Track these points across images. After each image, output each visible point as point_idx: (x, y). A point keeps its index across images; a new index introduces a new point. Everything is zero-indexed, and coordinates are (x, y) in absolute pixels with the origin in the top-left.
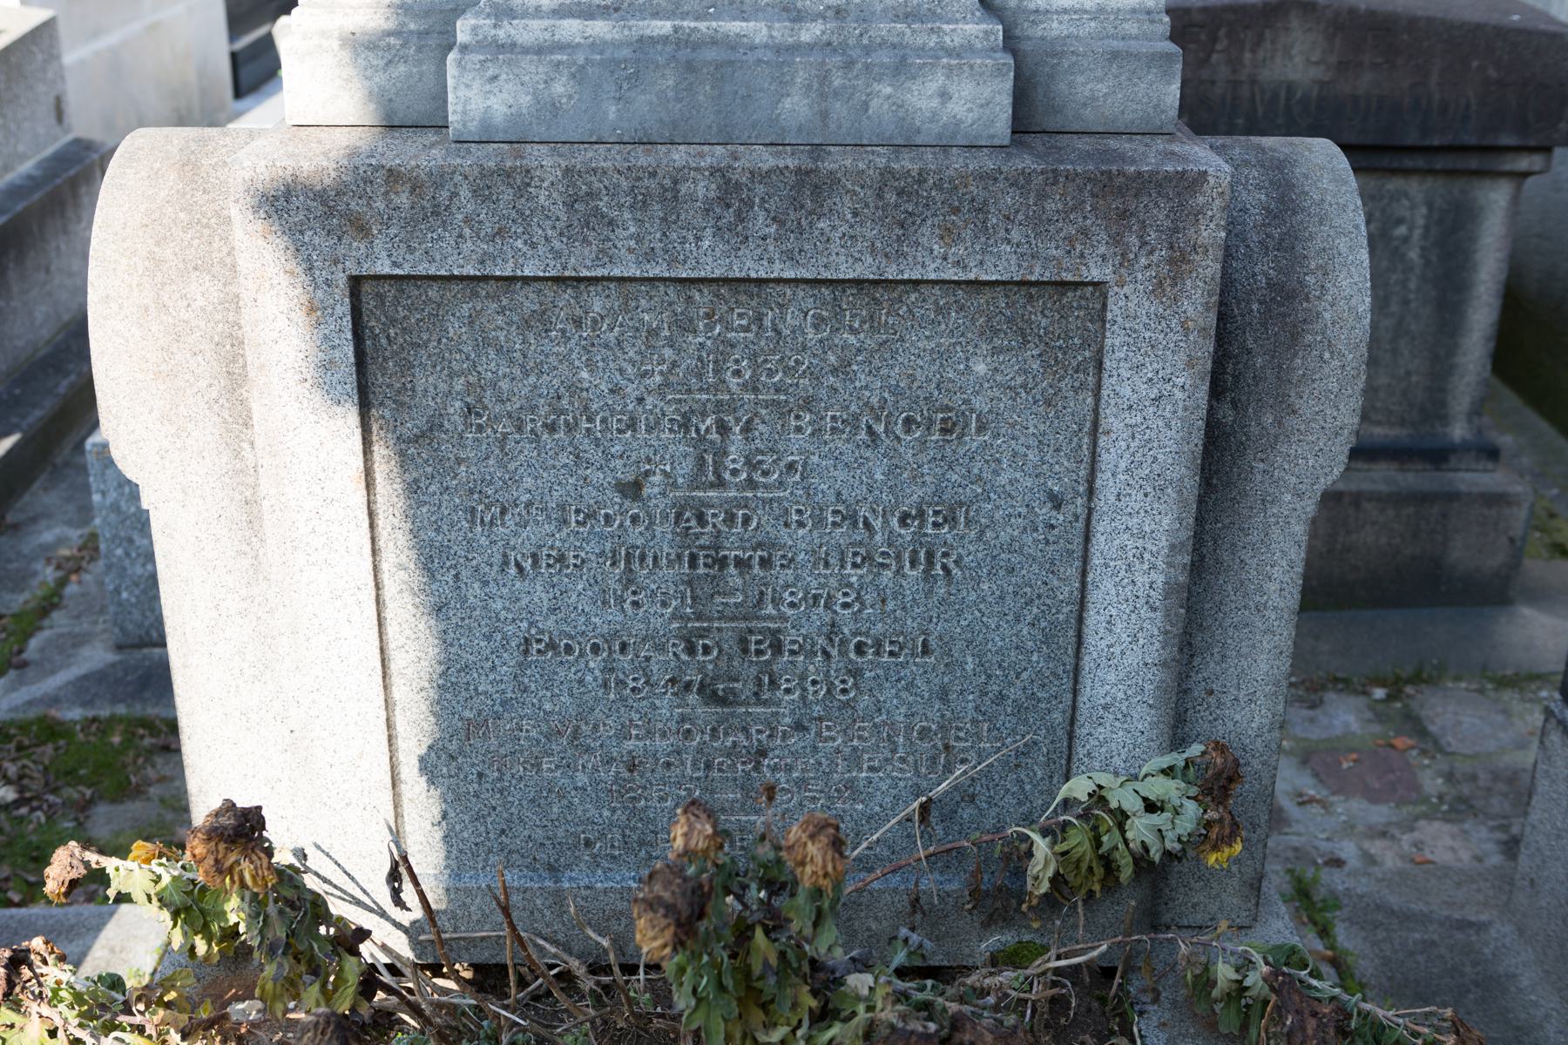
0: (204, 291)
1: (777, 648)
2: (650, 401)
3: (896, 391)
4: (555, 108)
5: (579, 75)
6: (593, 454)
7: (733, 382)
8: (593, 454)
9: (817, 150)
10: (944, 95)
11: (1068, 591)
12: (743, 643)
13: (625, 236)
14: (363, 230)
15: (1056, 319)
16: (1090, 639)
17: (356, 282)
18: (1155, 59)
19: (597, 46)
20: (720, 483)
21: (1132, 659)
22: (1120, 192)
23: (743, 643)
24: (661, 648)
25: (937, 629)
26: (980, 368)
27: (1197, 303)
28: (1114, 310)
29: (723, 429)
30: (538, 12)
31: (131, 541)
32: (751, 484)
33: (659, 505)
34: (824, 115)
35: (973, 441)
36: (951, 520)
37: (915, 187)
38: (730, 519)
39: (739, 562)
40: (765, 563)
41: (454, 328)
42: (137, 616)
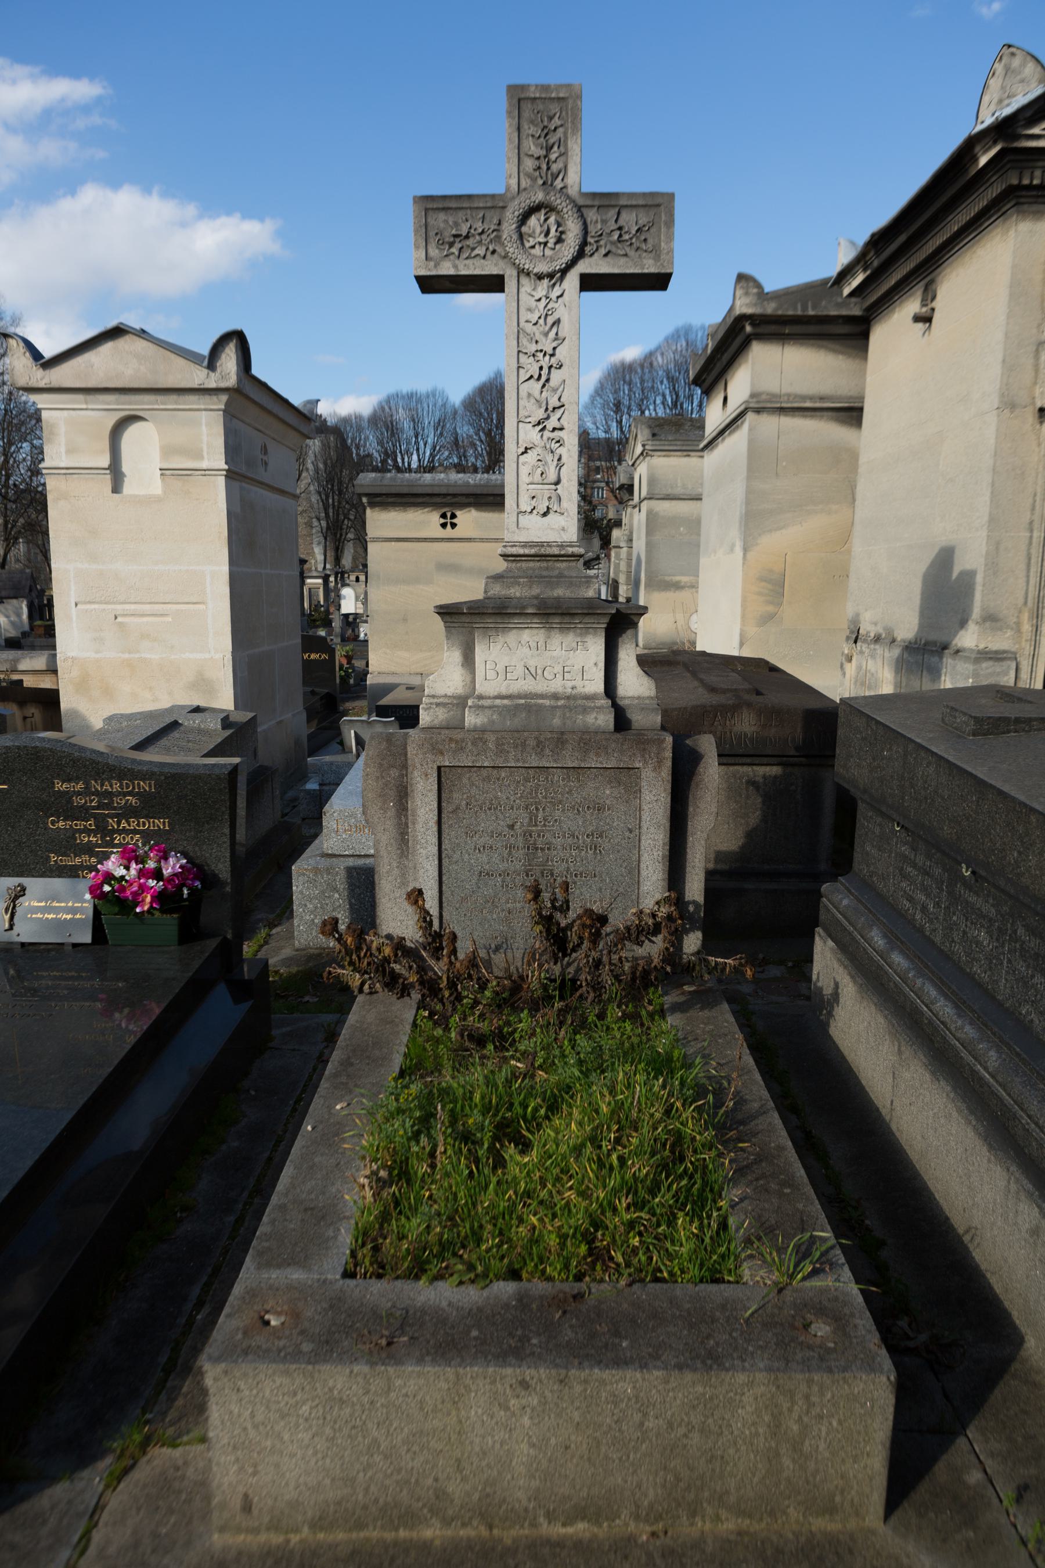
0: (394, 773)
1: (552, 875)
2: (518, 801)
3: (585, 799)
4: (493, 722)
5: (500, 714)
6: (501, 816)
7: (540, 796)
8: (501, 816)
9: (562, 733)
10: (596, 718)
11: (635, 858)
12: (542, 873)
13: (511, 755)
14: (442, 753)
15: (626, 778)
16: (642, 872)
17: (439, 768)
18: (653, 710)
19: (505, 706)
20: (536, 825)
21: (654, 878)
22: (643, 743)
23: (542, 873)
24: (519, 875)
25: (598, 869)
26: (608, 792)
27: (666, 772)
28: (643, 776)
29: (537, 809)
30: (489, 698)
31: (306, 905)
32: (545, 825)
33: (519, 831)
34: (564, 724)
35: (607, 813)
36: (601, 836)
37: (588, 740)
38: (539, 836)
39: (541, 849)
40: (549, 849)
41: (465, 781)
42: (305, 936)
